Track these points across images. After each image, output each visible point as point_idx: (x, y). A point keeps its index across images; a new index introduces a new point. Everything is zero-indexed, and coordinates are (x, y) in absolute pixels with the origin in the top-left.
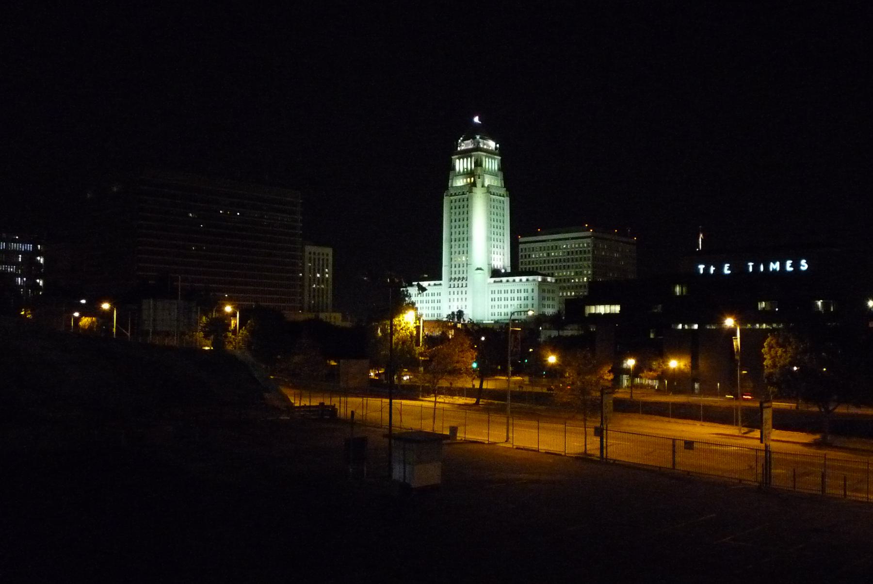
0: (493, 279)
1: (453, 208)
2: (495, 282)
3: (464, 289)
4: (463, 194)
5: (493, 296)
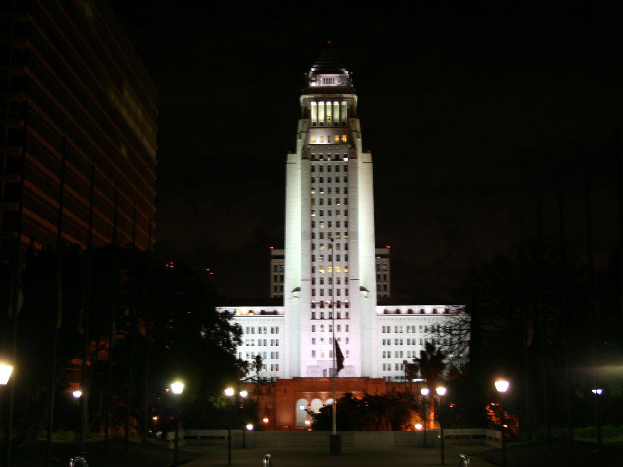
0: (381, 309)
1: (317, 180)
2: (386, 312)
3: (343, 323)
4: (337, 158)
5: (386, 336)
